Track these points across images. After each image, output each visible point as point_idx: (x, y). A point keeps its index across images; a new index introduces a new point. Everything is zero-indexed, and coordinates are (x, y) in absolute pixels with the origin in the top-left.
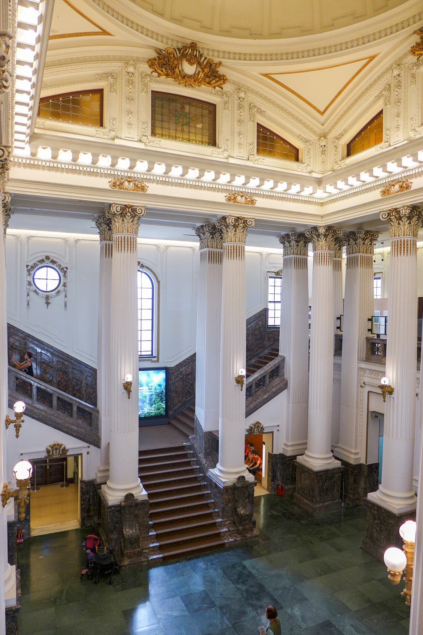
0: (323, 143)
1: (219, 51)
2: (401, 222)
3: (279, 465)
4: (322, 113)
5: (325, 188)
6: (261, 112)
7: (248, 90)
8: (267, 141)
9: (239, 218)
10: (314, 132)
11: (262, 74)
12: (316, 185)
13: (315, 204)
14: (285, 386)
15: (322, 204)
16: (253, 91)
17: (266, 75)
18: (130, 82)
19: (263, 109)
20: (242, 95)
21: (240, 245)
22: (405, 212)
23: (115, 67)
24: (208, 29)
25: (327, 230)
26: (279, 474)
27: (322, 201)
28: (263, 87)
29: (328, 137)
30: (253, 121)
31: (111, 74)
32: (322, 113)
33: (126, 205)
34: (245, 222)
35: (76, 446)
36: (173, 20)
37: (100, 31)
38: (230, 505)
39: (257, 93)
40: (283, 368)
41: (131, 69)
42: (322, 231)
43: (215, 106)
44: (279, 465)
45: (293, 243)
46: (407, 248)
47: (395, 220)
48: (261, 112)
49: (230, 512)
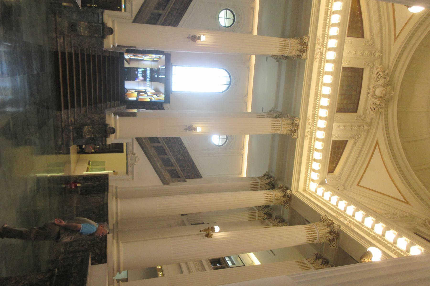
0: (340, 188)
2: (327, 226)
3: (98, 183)
4: (358, 185)
5: (320, 187)
6: (355, 143)
7: (368, 131)
9: (298, 126)
10: (345, 182)
11: (377, 140)
12: (320, 182)
13: (304, 185)
14: (165, 182)
16: (367, 135)
17: (377, 143)
20: (365, 128)
21: (281, 128)
25: (288, 196)
26: (89, 183)
27: (307, 189)
28: (371, 141)
29: (345, 191)
30: (351, 137)
31: (374, 42)
33: (307, 45)
34: (295, 131)
35: (133, 8)
37: (397, 34)
38: (89, 122)
39: (366, 138)
40: (178, 181)
42: (288, 192)
44: (98, 183)
45: (268, 181)
46: (311, 234)
49: (82, 122)
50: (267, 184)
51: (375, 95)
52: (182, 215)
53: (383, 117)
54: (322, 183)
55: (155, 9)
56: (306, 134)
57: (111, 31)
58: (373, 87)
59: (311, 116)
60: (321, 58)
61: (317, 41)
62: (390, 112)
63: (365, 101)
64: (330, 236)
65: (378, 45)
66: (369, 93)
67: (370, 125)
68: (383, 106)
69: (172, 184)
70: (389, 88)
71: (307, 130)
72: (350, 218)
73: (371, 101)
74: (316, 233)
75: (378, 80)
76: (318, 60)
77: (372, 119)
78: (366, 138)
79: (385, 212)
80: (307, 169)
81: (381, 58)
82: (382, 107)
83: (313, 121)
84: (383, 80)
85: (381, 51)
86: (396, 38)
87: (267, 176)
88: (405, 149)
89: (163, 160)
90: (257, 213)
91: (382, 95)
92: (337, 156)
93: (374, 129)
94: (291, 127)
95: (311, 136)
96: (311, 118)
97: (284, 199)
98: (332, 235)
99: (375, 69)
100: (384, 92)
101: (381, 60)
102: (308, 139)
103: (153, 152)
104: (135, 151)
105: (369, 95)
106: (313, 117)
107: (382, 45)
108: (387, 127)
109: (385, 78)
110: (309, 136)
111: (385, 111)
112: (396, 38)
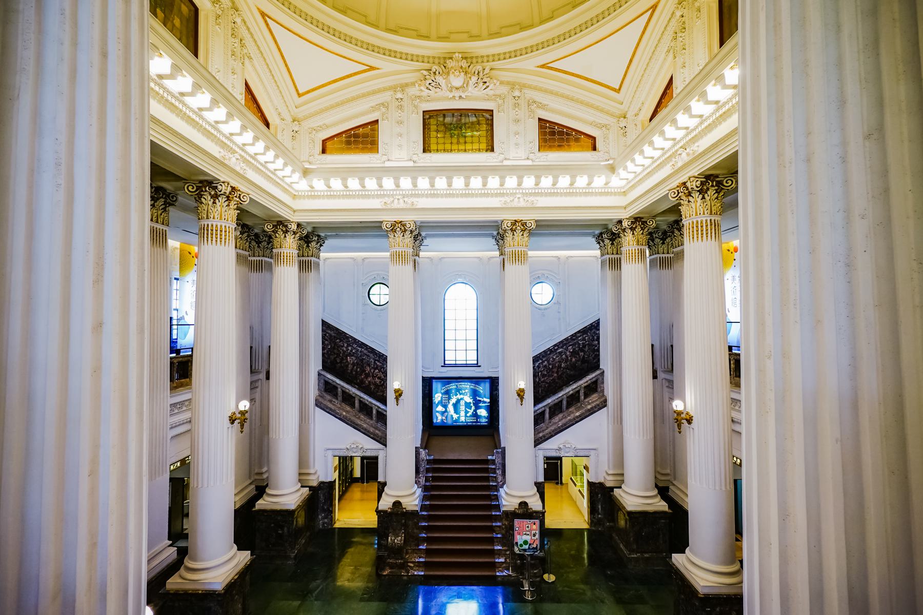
0: (622, 125)
1: (482, 57)
2: (691, 199)
4: (618, 91)
7: (523, 86)
8: (554, 135)
10: (612, 115)
14: (604, 404)
15: (624, 193)
16: (530, 87)
17: (543, 66)
18: (400, 107)
19: (546, 103)
22: (693, 185)
23: (387, 96)
24: (473, 37)
31: (383, 104)
32: (618, 91)
34: (524, 224)
36: (441, 38)
39: (535, 88)
40: (603, 383)
41: (399, 95)
43: (492, 111)
47: (684, 198)
48: (543, 107)
50: (612, 244)
51: (462, 87)
52: (655, 377)
53: (496, 64)
54: (612, 169)
55: (371, 418)
56: (529, 205)
57: (397, 504)
58: (451, 91)
59: (499, 199)
60: (412, 195)
61: (389, 207)
62: (491, 51)
63: (474, 98)
64: (709, 193)
65: (387, 96)
66: (460, 97)
67: (512, 85)
68: (479, 67)
69: (605, 393)
70: (450, 64)
71: (522, 204)
72: (678, 146)
73: (472, 91)
74: (702, 222)
75: (438, 86)
76: (415, 200)
77: (502, 83)
78: (535, 88)
79: (671, 55)
80: (586, 194)
81: (403, 87)
82: (481, 69)
83: (507, 194)
84: (437, 77)
85: (394, 88)
86: (372, 68)
87: (599, 238)
88: (551, 18)
89: (569, 405)
90: (661, 255)
91: (462, 74)
92: (568, 134)
93: (521, 75)
94: (518, 233)
95: (531, 194)
96: (503, 199)
97: (638, 230)
98: (708, 189)
99: (422, 94)
100: (457, 73)
101: (407, 85)
102: (537, 198)
103: (559, 420)
104: (556, 447)
105: (463, 96)
106: (502, 195)
107: (385, 90)
108: (515, 54)
109: (435, 73)
110: (531, 199)
111: (488, 61)
112: (372, 68)
